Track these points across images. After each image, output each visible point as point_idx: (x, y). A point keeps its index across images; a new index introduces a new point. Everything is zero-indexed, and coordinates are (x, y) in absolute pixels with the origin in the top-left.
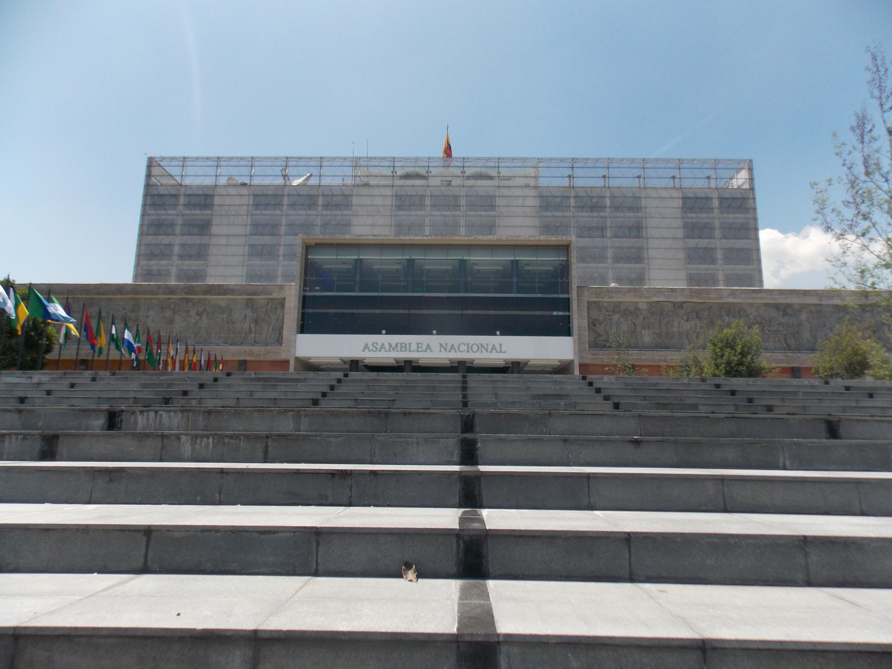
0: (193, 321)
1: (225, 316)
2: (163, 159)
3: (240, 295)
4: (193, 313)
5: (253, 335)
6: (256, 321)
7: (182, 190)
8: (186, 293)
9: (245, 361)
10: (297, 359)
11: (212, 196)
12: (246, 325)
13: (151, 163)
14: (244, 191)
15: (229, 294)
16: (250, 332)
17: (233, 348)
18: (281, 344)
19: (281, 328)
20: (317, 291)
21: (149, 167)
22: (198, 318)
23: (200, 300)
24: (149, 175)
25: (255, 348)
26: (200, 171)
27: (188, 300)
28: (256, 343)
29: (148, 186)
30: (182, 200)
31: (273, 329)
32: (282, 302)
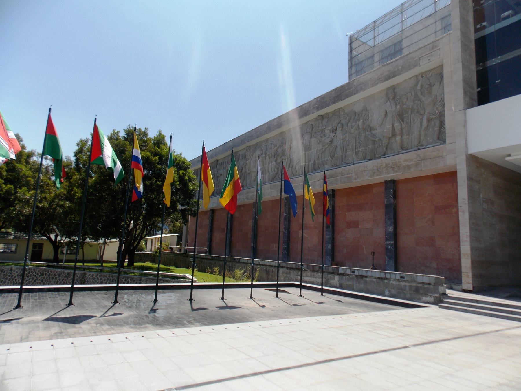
0: (328, 140)
1: (360, 123)
2: (358, 32)
3: (374, 85)
4: (327, 131)
5: (398, 138)
6: (401, 116)
7: (376, 50)
8: (318, 108)
9: (393, 182)
10: (474, 161)
11: (401, 42)
12: (388, 126)
13: (352, 41)
14: (431, 21)
15: (362, 89)
16: (394, 135)
17: (370, 164)
18: (444, 142)
19: (442, 115)
20: (508, 17)
21: (351, 44)
22: (332, 135)
23: (334, 113)
24: (351, 50)
25: (403, 158)
26: (387, 26)
27: (322, 117)
28: (403, 148)
29: (351, 59)
30: (377, 58)
31: (429, 120)
32: (438, 74)
